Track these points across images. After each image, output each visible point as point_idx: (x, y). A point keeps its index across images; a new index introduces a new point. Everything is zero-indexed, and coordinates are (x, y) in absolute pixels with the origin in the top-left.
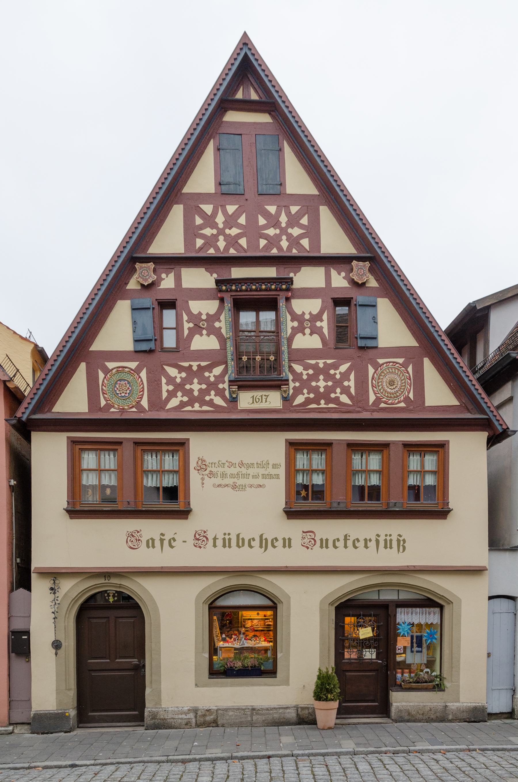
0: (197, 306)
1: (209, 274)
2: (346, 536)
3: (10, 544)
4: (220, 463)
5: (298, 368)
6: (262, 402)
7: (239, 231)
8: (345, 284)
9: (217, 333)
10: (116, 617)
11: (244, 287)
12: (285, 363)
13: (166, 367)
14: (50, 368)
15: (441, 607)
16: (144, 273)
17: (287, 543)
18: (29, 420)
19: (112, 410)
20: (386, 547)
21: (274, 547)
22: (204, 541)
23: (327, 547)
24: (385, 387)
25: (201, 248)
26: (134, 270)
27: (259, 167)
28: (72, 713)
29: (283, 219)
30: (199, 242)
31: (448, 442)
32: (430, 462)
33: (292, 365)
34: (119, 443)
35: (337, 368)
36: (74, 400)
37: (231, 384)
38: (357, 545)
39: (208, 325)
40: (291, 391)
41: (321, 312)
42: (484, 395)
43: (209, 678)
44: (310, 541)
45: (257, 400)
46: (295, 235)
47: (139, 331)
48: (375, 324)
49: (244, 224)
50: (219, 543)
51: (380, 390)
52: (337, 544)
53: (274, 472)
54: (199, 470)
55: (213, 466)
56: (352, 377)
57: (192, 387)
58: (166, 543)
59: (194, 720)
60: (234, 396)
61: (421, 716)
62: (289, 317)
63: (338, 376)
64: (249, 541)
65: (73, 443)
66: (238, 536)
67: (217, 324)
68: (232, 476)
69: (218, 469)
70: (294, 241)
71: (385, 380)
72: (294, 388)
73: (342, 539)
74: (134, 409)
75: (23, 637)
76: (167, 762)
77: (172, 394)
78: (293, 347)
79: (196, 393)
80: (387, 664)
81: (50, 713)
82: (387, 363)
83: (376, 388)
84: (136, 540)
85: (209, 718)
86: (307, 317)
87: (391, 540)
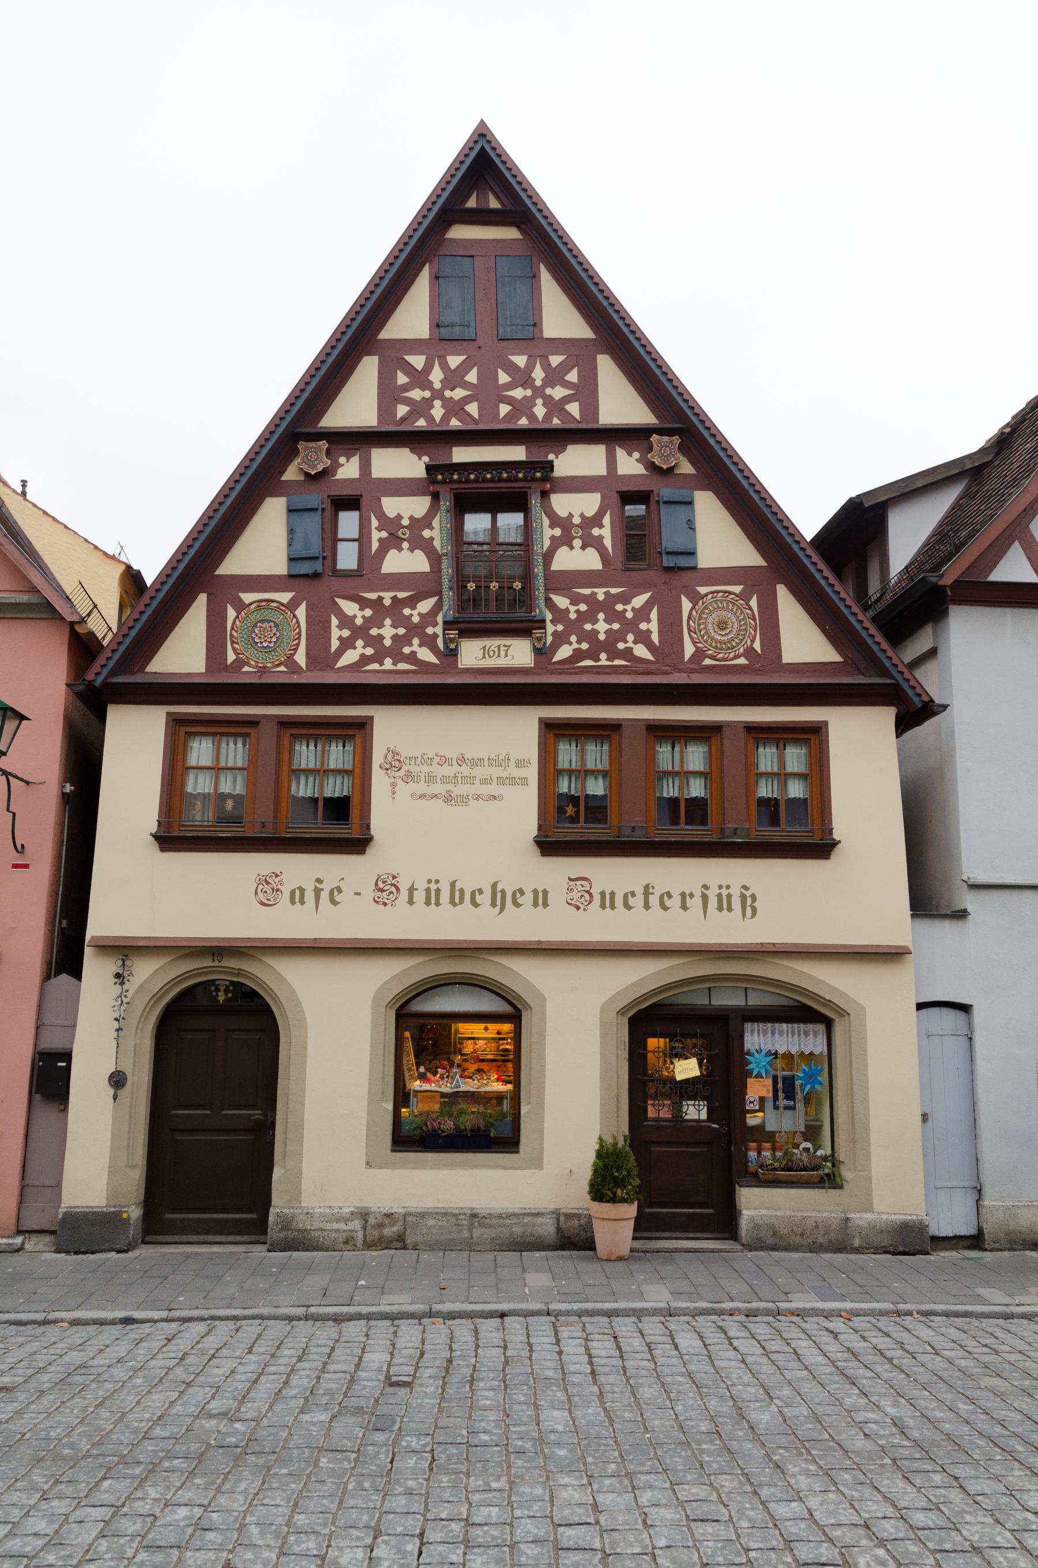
0: (391, 506)
1: (416, 457)
2: (647, 887)
3: (53, 894)
4: (425, 757)
5: (561, 602)
6: (499, 656)
7: (465, 393)
8: (640, 469)
9: (426, 546)
11: (472, 476)
12: (540, 593)
13: (339, 601)
14: (148, 601)
15: (828, 1023)
16: (312, 457)
18: (105, 684)
19: (246, 669)
20: (720, 908)
21: (517, 905)
22: (391, 892)
23: (613, 907)
24: (712, 631)
25: (404, 419)
26: (296, 452)
27: (500, 301)
28: (135, 1213)
29: (538, 374)
30: (402, 410)
31: (826, 723)
32: (795, 758)
33: (552, 596)
34: (253, 723)
36: (184, 653)
37: (448, 627)
38: (668, 903)
39: (413, 534)
40: (549, 639)
42: (885, 645)
43: (393, 1151)
45: (491, 653)
46: (557, 397)
47: (298, 545)
48: (690, 531)
49: (475, 382)
50: (419, 896)
51: (702, 637)
52: (631, 901)
53: (518, 773)
54: (387, 769)
55: (413, 762)
56: (654, 615)
57: (382, 631)
58: (325, 896)
59: (360, 1235)
60: (452, 646)
61: (798, 1239)
62: (546, 522)
63: (629, 615)
64: (473, 893)
65: (175, 723)
66: (453, 885)
67: (426, 533)
68: (445, 780)
70: (556, 407)
71: (710, 620)
72: (555, 634)
74: (282, 668)
76: (307, 1318)
77: (347, 644)
78: (552, 568)
79: (387, 642)
80: (729, 1132)
82: (713, 593)
84: (273, 889)
86: (577, 520)
87: (729, 896)
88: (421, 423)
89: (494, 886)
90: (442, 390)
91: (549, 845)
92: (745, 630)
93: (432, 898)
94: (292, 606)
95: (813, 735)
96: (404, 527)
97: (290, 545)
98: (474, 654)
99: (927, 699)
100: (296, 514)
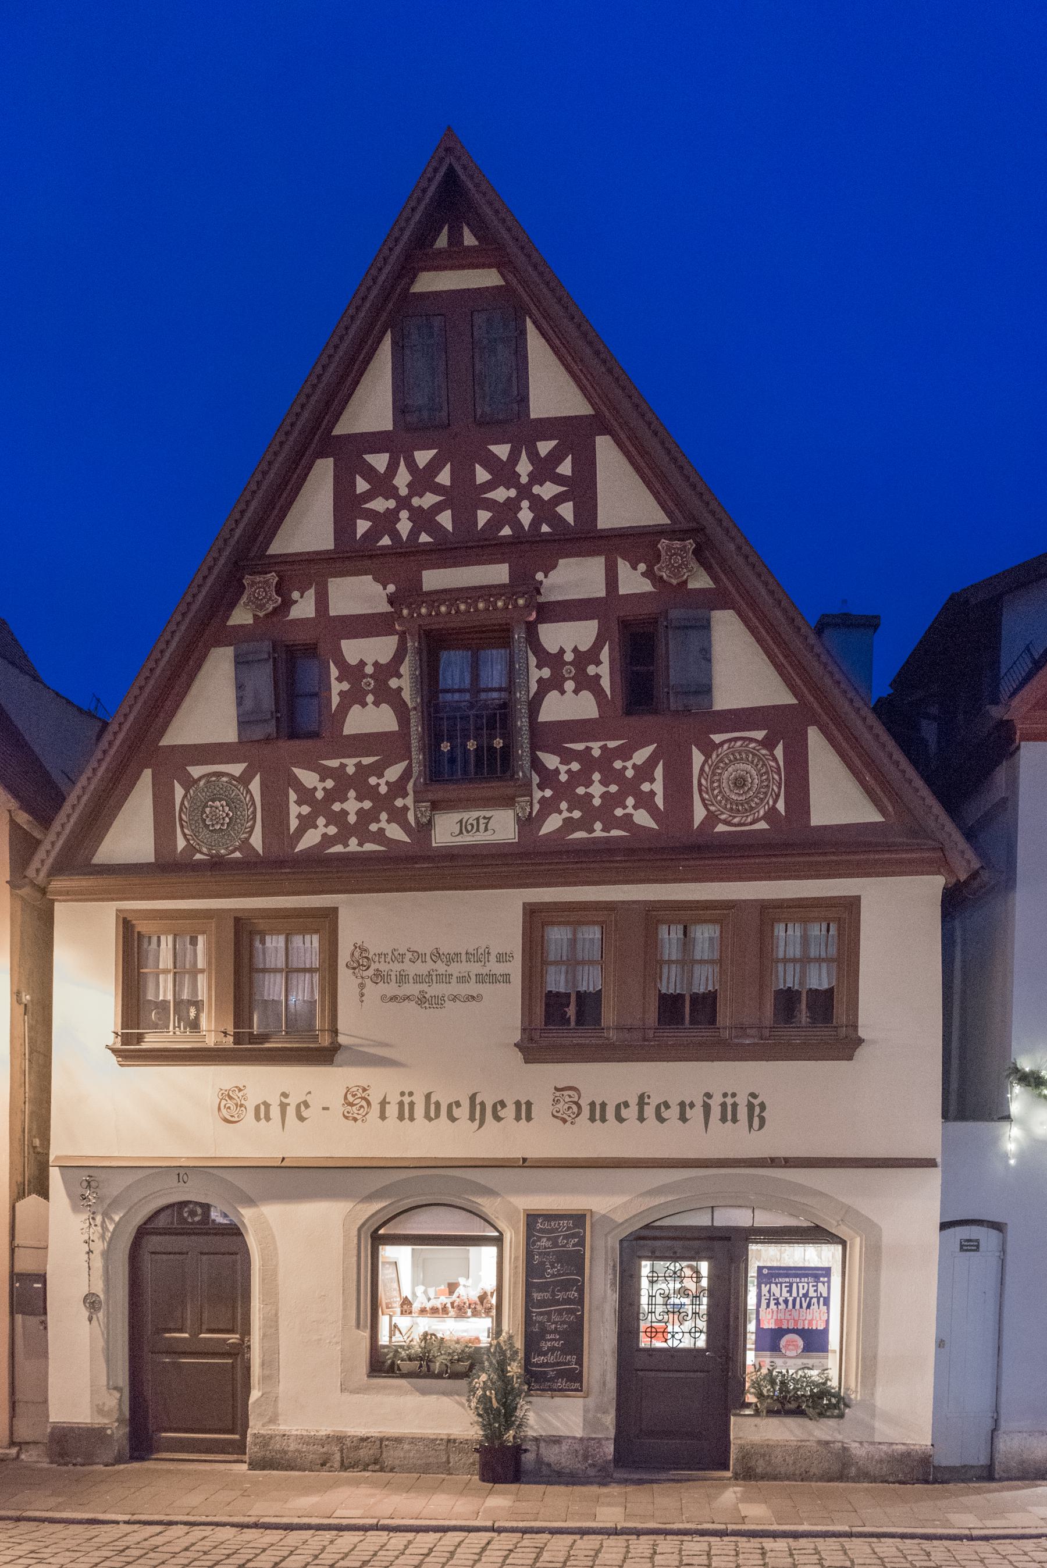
0: (353, 650)
2: (641, 1097)
4: (396, 953)
5: (551, 761)
6: (478, 830)
9: (393, 699)
12: (523, 751)
20: (724, 1119)
21: (498, 1119)
22: (362, 1107)
23: (603, 1119)
29: (524, 468)
30: (363, 526)
38: (665, 1114)
40: (536, 807)
41: (597, 646)
44: (569, 1108)
46: (546, 497)
49: (448, 483)
50: (392, 1110)
52: (624, 1113)
53: (499, 969)
54: (354, 968)
56: (659, 772)
57: (345, 806)
58: (291, 1111)
59: (338, 1456)
62: (533, 661)
63: (630, 773)
66: (428, 1097)
67: (394, 683)
68: (418, 979)
69: (392, 966)
72: (543, 801)
73: (633, 1102)
75: (36, 1285)
77: (307, 823)
79: (352, 819)
81: (79, 1428)
83: (707, 793)
84: (237, 1105)
85: (364, 1454)
86: (569, 657)
87: (735, 1106)
89: (473, 1098)
90: (410, 496)
92: (768, 786)
94: (245, 780)
98: (447, 830)
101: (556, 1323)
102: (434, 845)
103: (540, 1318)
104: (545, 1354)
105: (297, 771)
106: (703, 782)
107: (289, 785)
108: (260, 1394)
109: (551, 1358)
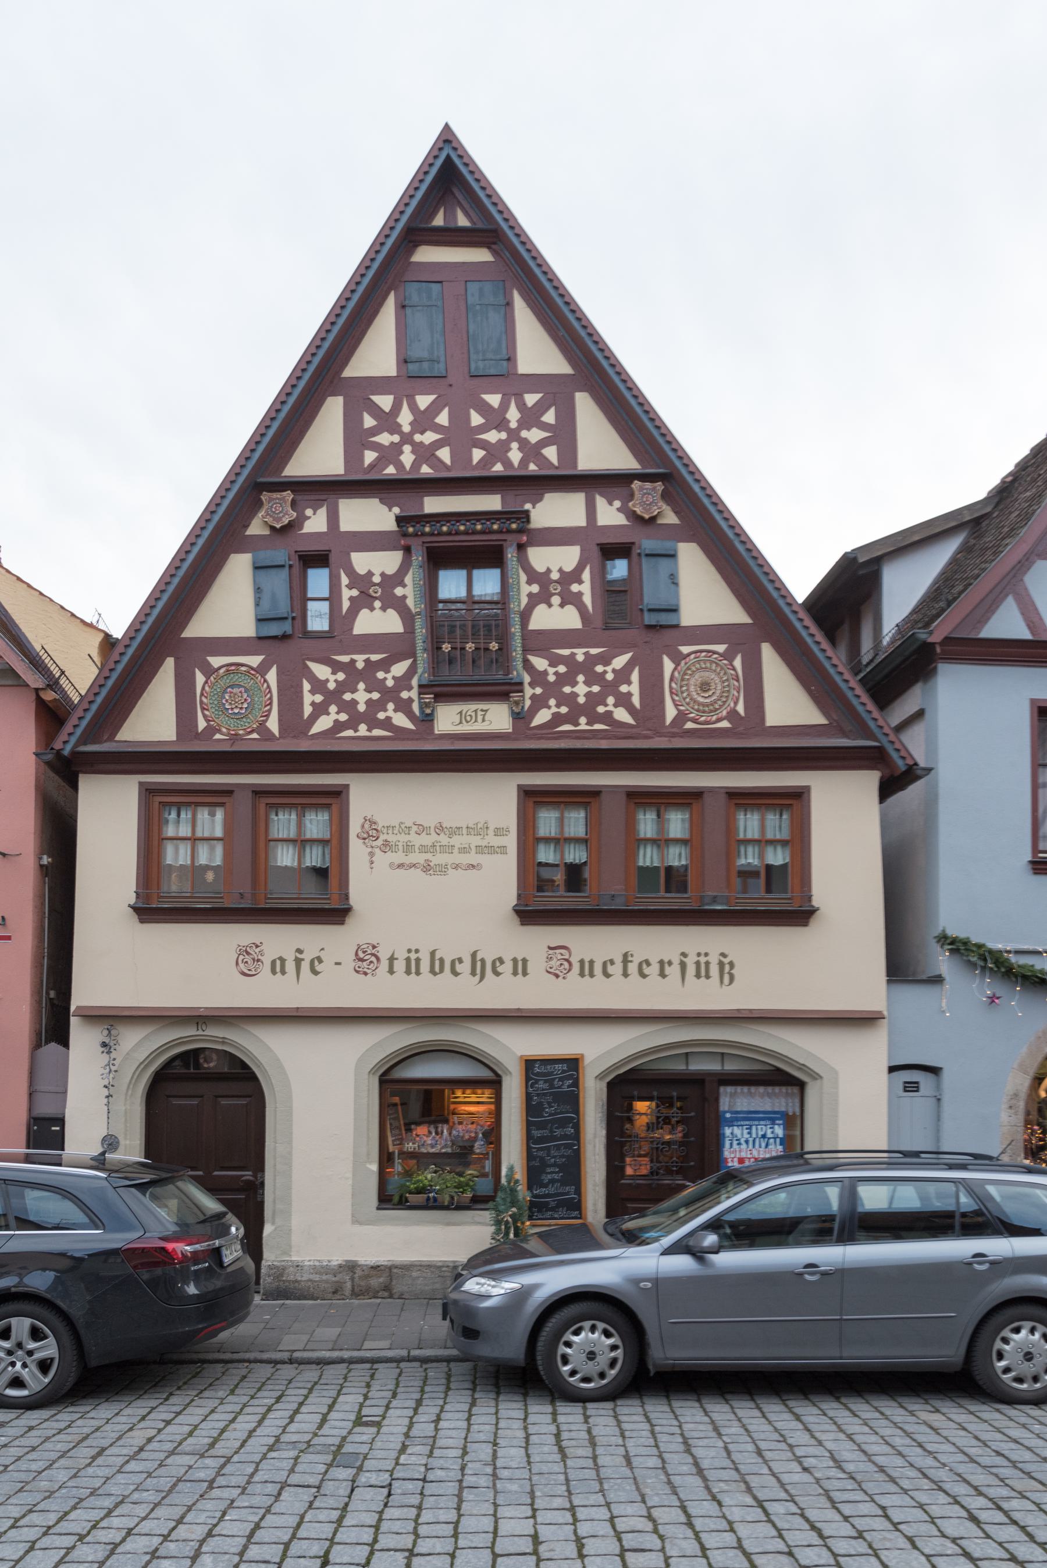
0: (363, 561)
1: (385, 508)
2: (625, 955)
4: (403, 826)
5: (540, 663)
6: (476, 721)
7: (438, 437)
8: (621, 520)
9: (399, 605)
10: (217, 1097)
12: (517, 653)
13: (310, 664)
16: (277, 508)
17: (520, 967)
18: (74, 753)
19: (218, 736)
20: (698, 976)
21: (497, 974)
22: (371, 962)
23: (592, 975)
25: (372, 466)
26: (259, 504)
29: (513, 415)
30: (370, 457)
32: (776, 825)
33: (531, 658)
34: (227, 792)
35: (607, 663)
36: (153, 721)
37: (423, 690)
38: (646, 970)
40: (528, 703)
43: (378, 1209)
45: (468, 718)
47: (266, 604)
48: (673, 586)
50: (400, 966)
52: (610, 969)
54: (364, 839)
55: (390, 831)
56: (635, 676)
57: (355, 696)
58: (305, 966)
59: (349, 1285)
60: (428, 711)
62: (523, 577)
63: (610, 676)
64: (453, 962)
65: (148, 792)
66: (433, 954)
67: (399, 591)
68: (423, 849)
70: (532, 451)
71: (692, 681)
72: (533, 697)
74: (255, 736)
77: (320, 710)
79: (362, 708)
84: (254, 960)
85: (376, 1282)
86: (555, 576)
87: (707, 963)
88: (391, 470)
89: (474, 955)
91: (528, 915)
93: (412, 967)
95: (795, 801)
96: (375, 585)
97: (257, 605)
98: (450, 720)
99: (911, 763)
100: (262, 572)
101: (554, 1157)
102: (436, 732)
103: (541, 1153)
104: (546, 1186)
105: (311, 665)
106: (674, 685)
107: (304, 676)
108: (273, 1228)
109: (551, 1190)
